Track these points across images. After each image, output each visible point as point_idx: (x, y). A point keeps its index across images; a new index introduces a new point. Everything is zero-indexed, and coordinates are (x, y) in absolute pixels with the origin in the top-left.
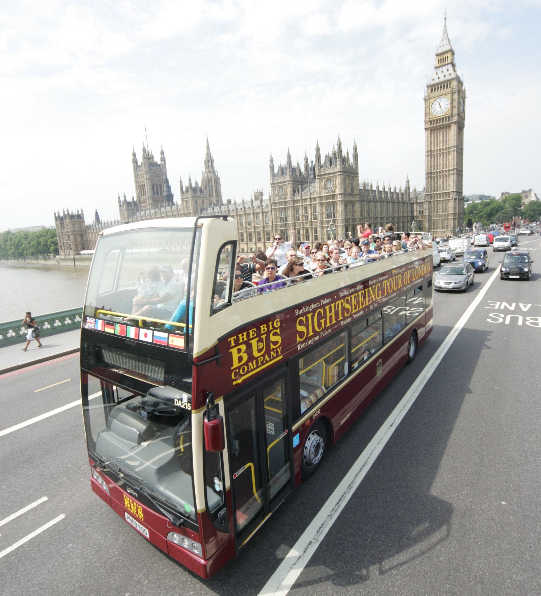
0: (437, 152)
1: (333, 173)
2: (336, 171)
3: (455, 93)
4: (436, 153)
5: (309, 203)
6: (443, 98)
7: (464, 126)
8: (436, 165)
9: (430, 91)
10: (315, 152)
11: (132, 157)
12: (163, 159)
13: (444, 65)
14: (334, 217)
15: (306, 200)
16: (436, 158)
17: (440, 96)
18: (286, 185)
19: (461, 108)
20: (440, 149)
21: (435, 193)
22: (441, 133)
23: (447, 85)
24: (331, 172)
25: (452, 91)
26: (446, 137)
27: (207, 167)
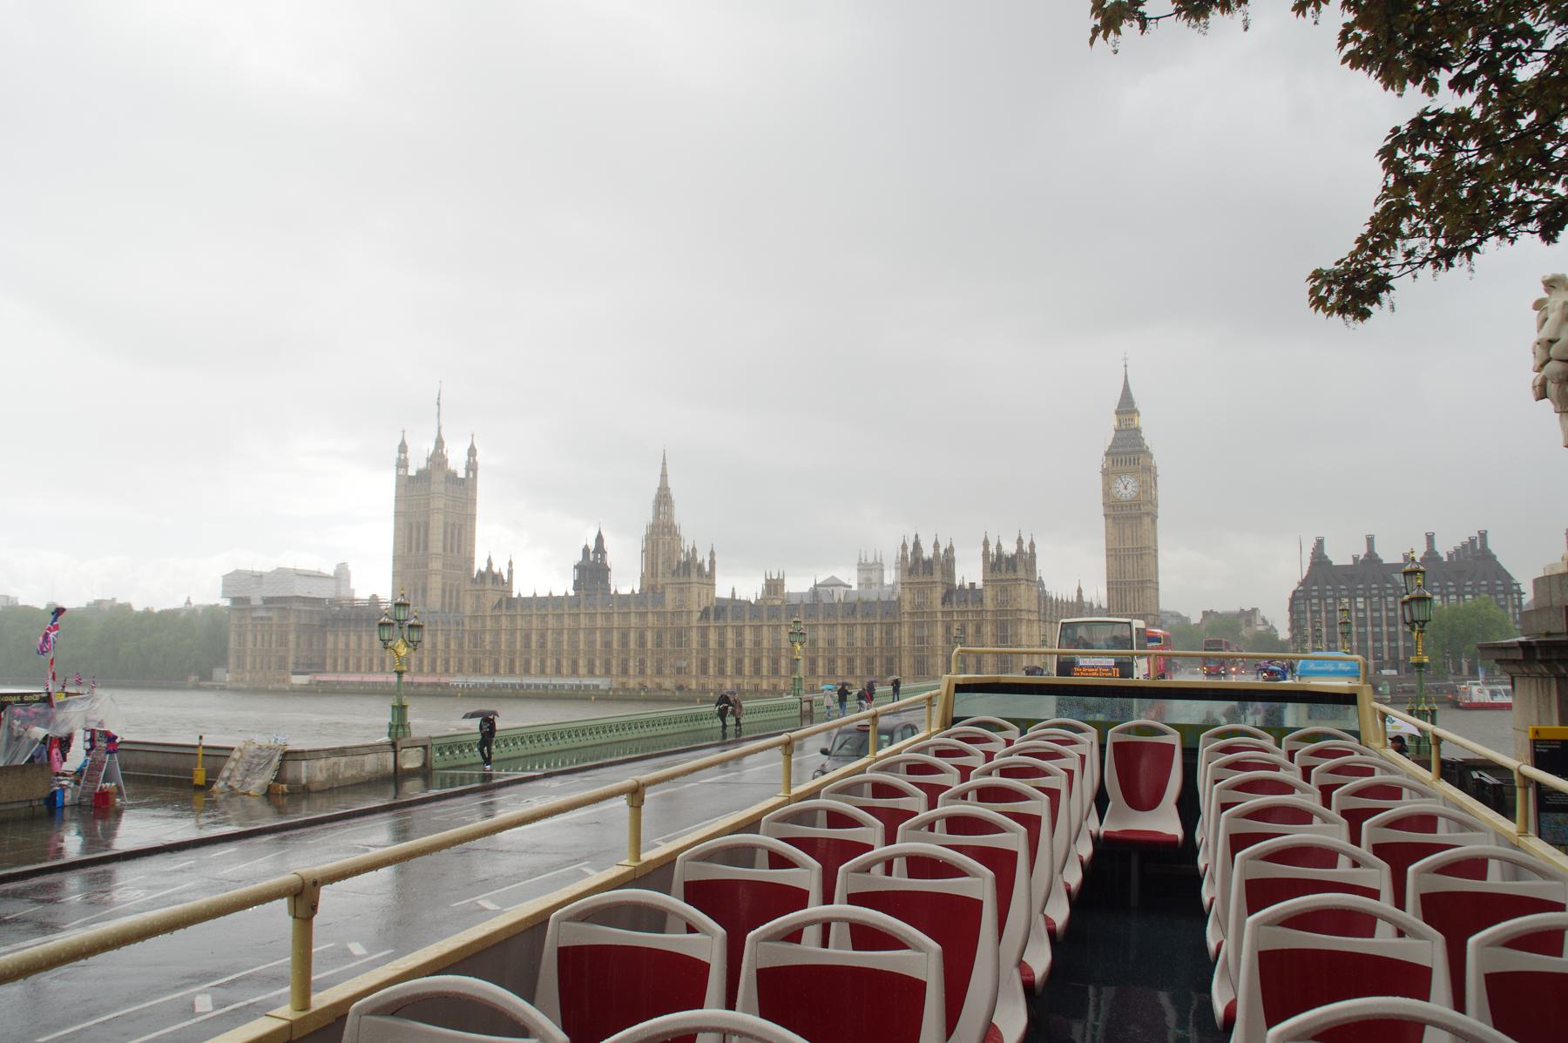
0: (1124, 551)
2: (1014, 577)
4: (1122, 553)
5: (970, 618)
7: (1157, 517)
9: (1111, 463)
10: (981, 549)
11: (395, 454)
12: (472, 467)
14: (1011, 642)
15: (961, 613)
16: (1122, 561)
17: (1125, 473)
19: (1154, 493)
23: (1134, 460)
27: (657, 513)
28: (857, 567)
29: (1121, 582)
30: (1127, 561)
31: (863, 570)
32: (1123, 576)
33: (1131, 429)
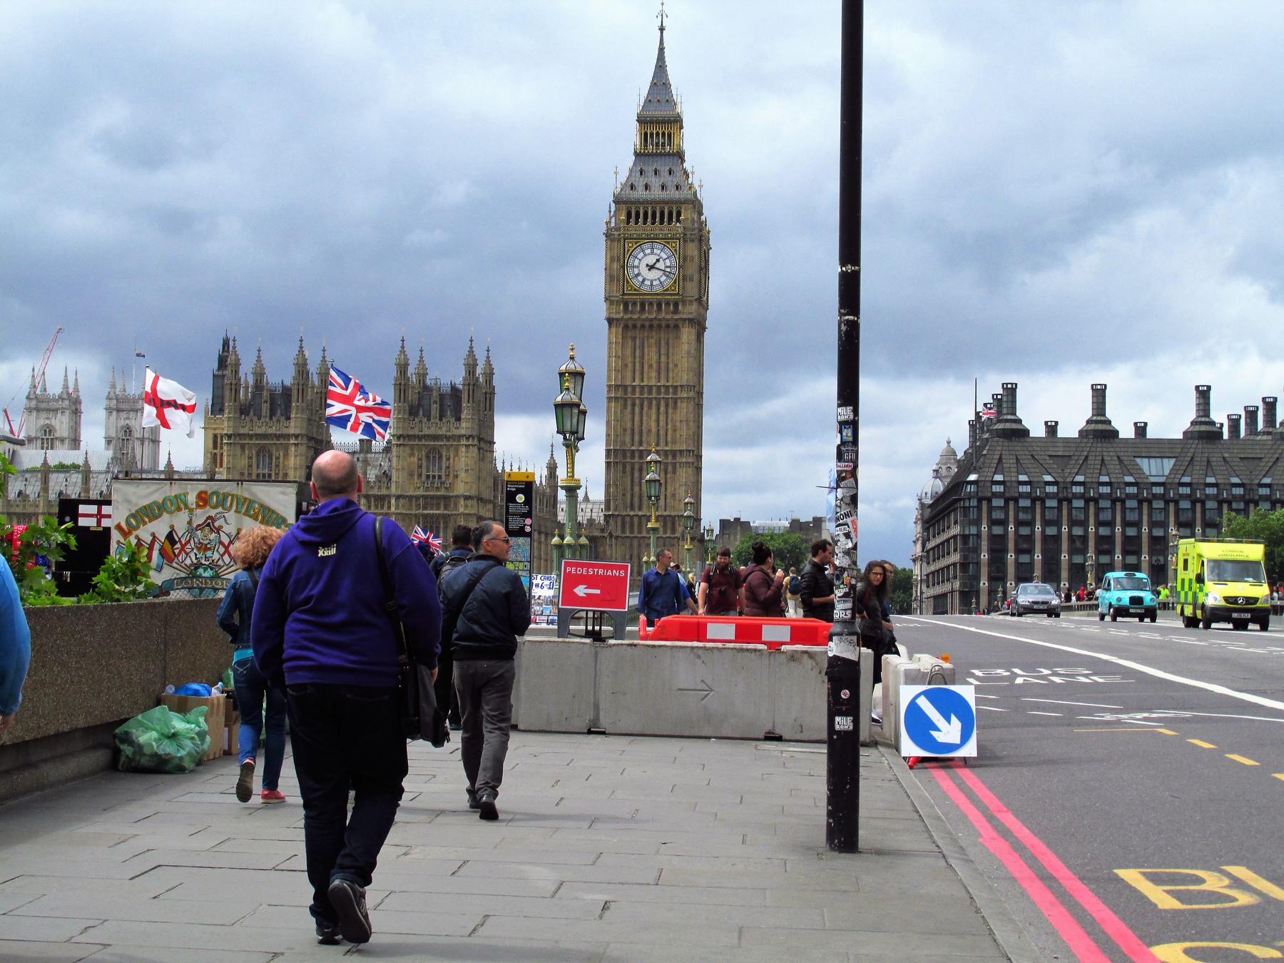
0: (642, 393)
1: (448, 438)
2: (456, 432)
3: (692, 241)
6: (660, 246)
7: (704, 329)
8: (637, 431)
9: (623, 217)
10: (394, 372)
13: (661, 155)
16: (637, 410)
17: (652, 239)
18: (286, 448)
20: (651, 386)
21: (632, 513)
22: (653, 341)
24: (440, 433)
25: (685, 235)
26: (668, 355)
28: (105, 403)
29: (633, 451)
30: (645, 409)
31: (38, 410)
32: (637, 438)
33: (669, 154)
